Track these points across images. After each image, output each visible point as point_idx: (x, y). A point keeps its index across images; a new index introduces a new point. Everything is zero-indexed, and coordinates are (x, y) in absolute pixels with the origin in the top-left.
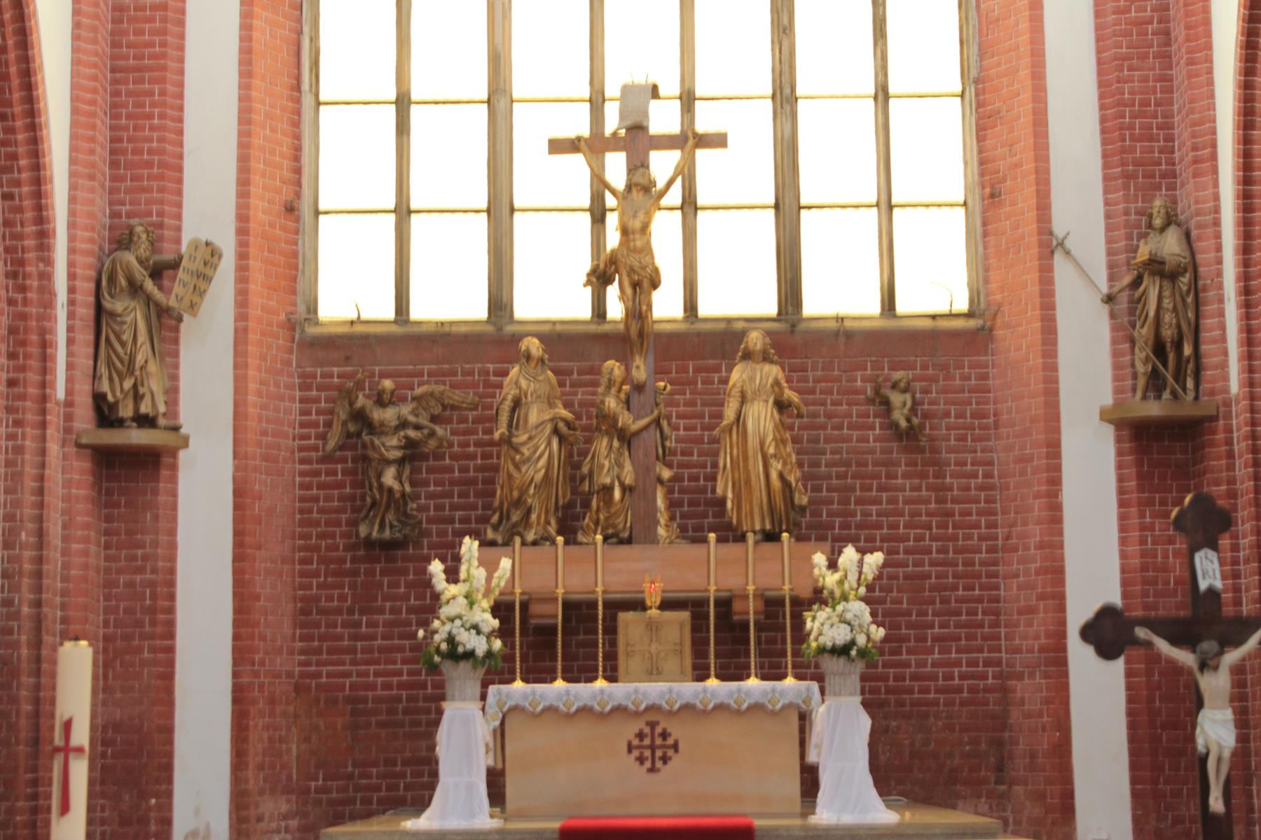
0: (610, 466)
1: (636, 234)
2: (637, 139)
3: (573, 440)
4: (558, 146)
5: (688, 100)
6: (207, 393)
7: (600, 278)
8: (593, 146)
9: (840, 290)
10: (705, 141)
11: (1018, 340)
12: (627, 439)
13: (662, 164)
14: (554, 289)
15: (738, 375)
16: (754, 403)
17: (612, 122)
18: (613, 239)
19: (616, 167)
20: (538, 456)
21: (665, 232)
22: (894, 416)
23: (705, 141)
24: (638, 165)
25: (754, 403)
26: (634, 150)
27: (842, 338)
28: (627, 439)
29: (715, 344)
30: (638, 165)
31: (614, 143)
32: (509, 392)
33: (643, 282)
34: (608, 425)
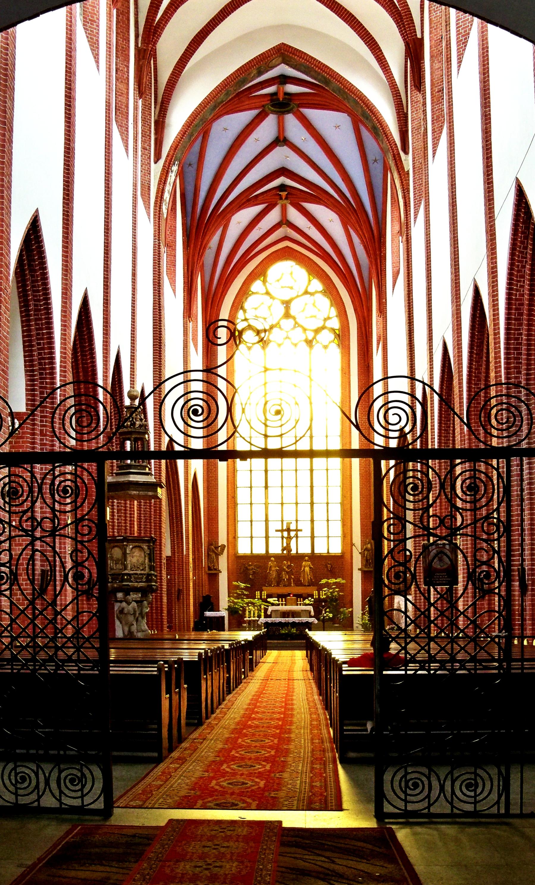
0: (285, 577)
1: (288, 544)
2: (289, 530)
3: (279, 573)
4: (277, 531)
5: (297, 521)
6: (223, 563)
7: (283, 550)
8: (282, 531)
9: (321, 549)
10: (299, 530)
11: (348, 556)
12: (287, 573)
13: (293, 534)
14: (276, 548)
15: (304, 563)
16: (306, 567)
17: (285, 528)
18: (285, 545)
19: (285, 534)
20: (274, 574)
21: (293, 541)
22: (331, 566)
23: (299, 530)
24: (289, 534)
25: (306, 567)
26: (288, 532)
27: (321, 557)
28: (287, 573)
29: (300, 557)
30: (289, 534)
31: (285, 530)
32: (269, 566)
33: (290, 550)
34: (284, 570)
